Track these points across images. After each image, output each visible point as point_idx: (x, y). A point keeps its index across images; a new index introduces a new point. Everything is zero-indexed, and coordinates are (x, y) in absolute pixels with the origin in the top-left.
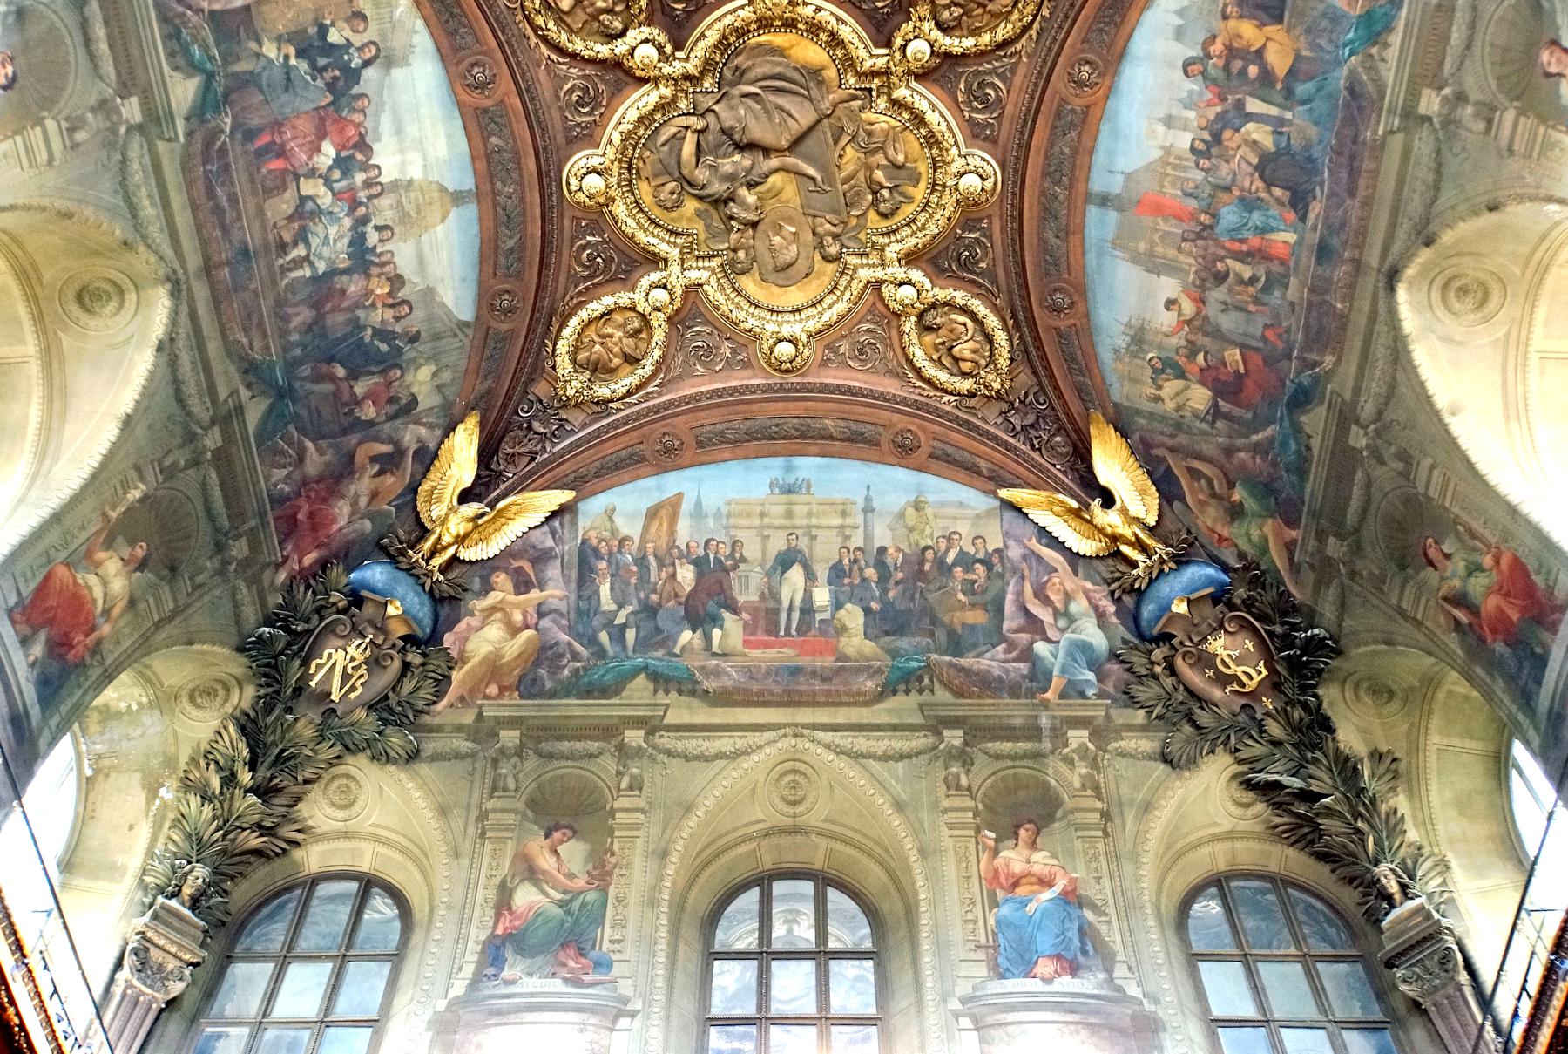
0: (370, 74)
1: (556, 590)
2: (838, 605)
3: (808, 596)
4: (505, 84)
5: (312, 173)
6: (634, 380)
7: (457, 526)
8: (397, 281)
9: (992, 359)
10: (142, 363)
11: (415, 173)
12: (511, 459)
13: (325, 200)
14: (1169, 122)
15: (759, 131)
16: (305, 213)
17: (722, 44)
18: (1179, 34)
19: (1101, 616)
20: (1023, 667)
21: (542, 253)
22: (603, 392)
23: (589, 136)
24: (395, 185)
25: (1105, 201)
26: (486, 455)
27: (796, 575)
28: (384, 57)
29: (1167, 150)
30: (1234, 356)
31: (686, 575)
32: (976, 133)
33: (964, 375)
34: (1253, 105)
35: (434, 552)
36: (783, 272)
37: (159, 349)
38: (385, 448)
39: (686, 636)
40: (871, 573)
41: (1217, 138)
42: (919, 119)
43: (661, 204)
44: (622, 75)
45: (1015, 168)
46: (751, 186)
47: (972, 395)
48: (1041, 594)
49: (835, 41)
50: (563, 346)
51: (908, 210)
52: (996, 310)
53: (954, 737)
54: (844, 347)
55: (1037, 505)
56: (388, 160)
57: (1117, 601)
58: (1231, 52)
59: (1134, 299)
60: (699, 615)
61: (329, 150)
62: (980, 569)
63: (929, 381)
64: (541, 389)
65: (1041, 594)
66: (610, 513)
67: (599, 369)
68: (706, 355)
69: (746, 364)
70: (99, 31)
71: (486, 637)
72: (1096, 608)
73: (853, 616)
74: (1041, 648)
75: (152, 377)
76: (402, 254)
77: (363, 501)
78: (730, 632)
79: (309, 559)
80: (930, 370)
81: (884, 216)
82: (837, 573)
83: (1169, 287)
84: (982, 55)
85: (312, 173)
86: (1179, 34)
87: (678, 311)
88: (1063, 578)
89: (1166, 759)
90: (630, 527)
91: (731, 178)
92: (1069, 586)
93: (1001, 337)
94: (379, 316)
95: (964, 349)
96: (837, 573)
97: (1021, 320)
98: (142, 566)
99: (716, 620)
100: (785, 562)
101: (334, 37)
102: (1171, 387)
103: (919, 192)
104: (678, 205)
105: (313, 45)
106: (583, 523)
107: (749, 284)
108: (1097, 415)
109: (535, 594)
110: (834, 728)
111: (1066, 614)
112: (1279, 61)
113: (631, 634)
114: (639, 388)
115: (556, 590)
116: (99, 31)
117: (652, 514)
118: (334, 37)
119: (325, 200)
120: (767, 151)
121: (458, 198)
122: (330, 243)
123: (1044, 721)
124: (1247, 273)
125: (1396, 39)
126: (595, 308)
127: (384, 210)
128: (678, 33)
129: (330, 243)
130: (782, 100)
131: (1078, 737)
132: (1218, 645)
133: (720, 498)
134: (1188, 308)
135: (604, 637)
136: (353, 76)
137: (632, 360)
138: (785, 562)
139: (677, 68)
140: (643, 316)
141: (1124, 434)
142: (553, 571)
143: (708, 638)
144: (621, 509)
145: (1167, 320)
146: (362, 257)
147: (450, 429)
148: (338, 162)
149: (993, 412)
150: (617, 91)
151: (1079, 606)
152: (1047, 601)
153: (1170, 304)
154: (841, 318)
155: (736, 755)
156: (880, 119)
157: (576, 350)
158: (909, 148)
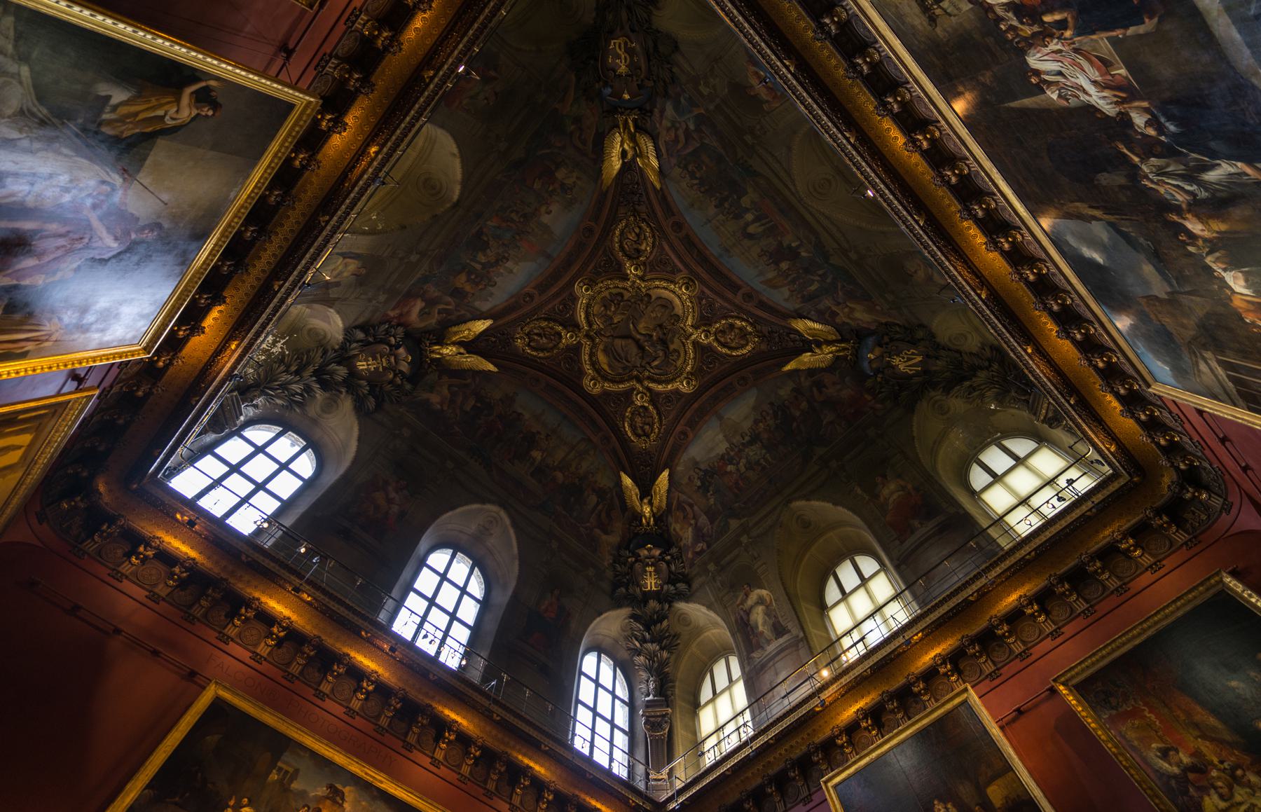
0: (702, 467)
1: (827, 302)
2: (747, 210)
3: (754, 221)
4: (679, 428)
5: (738, 470)
6: (738, 322)
7: (827, 349)
8: (756, 422)
9: (626, 226)
10: (816, 504)
11: (721, 436)
12: (794, 341)
13: (743, 461)
14: (511, 271)
15: (634, 350)
16: (750, 466)
17: (621, 382)
18: (491, 294)
19: (662, 111)
20: (704, 128)
21: (720, 380)
22: (749, 329)
23: (677, 391)
24: (728, 441)
25: (549, 256)
26: (798, 352)
27: (751, 229)
28: (696, 464)
29: (516, 264)
30: (537, 186)
31: (784, 266)
32: (574, 299)
33: (640, 228)
34: (478, 267)
35: (844, 349)
36: (667, 305)
37: (808, 500)
38: (815, 389)
39: (803, 254)
40: (726, 205)
41: (497, 262)
42: (587, 317)
43: (679, 356)
44: (654, 398)
45: (571, 284)
46: (651, 336)
47: (644, 220)
48: (676, 140)
49: (592, 355)
50: (745, 351)
51: (614, 291)
52: (612, 241)
53: (748, 138)
54: (669, 269)
55: (653, 168)
56: (723, 447)
57: (651, 112)
58: (477, 284)
59: (558, 220)
60: (793, 254)
61: (730, 468)
62: (690, 168)
63: (653, 236)
64: (763, 347)
65: (676, 140)
66: (786, 300)
67: (743, 334)
68: (711, 305)
69: (703, 292)
70: (728, 558)
71: (862, 316)
72: (661, 116)
73: (745, 202)
74: (692, 127)
75: (818, 500)
76: (747, 425)
77: (838, 387)
78: (790, 240)
79: (869, 397)
80: (650, 240)
81: (622, 295)
82: (738, 217)
83: (545, 219)
84: (555, 321)
85: (738, 470)
86: (491, 294)
87: (705, 325)
88: (665, 137)
89: (676, 48)
90: (785, 291)
91: (653, 345)
92: (664, 133)
93: (617, 232)
94: (771, 422)
95: (632, 237)
96: (738, 217)
97: (607, 231)
98: (884, 476)
99: (789, 247)
100: (751, 236)
101: (699, 483)
102: (569, 181)
103: (606, 294)
104: (675, 351)
105: (704, 488)
106: (797, 306)
107: (679, 310)
108: (604, 188)
109: (834, 308)
110: (786, 186)
111: (673, 125)
112: (463, 278)
113: (820, 272)
114: (738, 318)
115: (827, 302)
116: (728, 558)
117: (775, 287)
118: (699, 483)
119: (743, 461)
120: (637, 342)
121: (720, 418)
122: (754, 452)
123: (711, 107)
124: (513, 215)
125: (419, 276)
126: (724, 350)
127: (737, 439)
128: (628, 394)
129: (754, 452)
130: (620, 351)
131: (705, 91)
132: (623, 69)
133: (748, 269)
134: (543, 209)
135: (829, 280)
136: (706, 471)
137: (732, 326)
138: (751, 236)
139: (638, 386)
140: (715, 334)
141: (601, 170)
142: (821, 306)
143: (798, 247)
144: (781, 297)
145: (555, 208)
146: (755, 438)
147: (796, 371)
148: (731, 463)
149: (643, 208)
150: (659, 394)
151: (666, 123)
152: (676, 136)
153: (549, 213)
154: (661, 279)
155: (827, 218)
156: (598, 323)
157: (743, 347)
158: (596, 309)
